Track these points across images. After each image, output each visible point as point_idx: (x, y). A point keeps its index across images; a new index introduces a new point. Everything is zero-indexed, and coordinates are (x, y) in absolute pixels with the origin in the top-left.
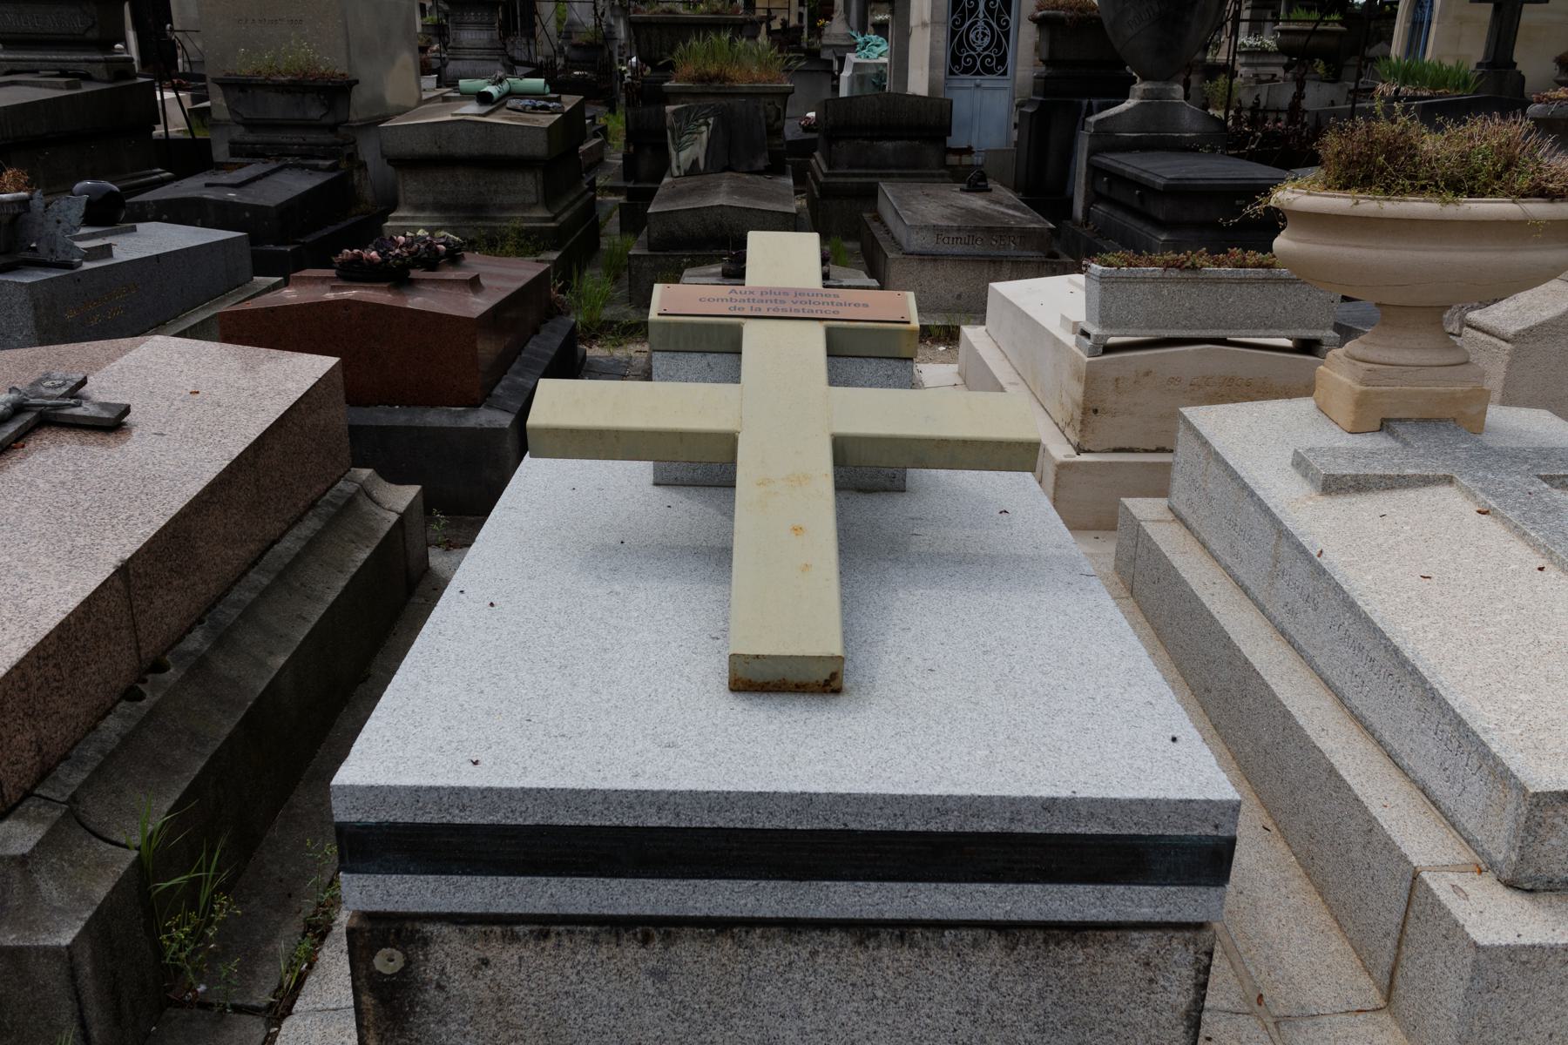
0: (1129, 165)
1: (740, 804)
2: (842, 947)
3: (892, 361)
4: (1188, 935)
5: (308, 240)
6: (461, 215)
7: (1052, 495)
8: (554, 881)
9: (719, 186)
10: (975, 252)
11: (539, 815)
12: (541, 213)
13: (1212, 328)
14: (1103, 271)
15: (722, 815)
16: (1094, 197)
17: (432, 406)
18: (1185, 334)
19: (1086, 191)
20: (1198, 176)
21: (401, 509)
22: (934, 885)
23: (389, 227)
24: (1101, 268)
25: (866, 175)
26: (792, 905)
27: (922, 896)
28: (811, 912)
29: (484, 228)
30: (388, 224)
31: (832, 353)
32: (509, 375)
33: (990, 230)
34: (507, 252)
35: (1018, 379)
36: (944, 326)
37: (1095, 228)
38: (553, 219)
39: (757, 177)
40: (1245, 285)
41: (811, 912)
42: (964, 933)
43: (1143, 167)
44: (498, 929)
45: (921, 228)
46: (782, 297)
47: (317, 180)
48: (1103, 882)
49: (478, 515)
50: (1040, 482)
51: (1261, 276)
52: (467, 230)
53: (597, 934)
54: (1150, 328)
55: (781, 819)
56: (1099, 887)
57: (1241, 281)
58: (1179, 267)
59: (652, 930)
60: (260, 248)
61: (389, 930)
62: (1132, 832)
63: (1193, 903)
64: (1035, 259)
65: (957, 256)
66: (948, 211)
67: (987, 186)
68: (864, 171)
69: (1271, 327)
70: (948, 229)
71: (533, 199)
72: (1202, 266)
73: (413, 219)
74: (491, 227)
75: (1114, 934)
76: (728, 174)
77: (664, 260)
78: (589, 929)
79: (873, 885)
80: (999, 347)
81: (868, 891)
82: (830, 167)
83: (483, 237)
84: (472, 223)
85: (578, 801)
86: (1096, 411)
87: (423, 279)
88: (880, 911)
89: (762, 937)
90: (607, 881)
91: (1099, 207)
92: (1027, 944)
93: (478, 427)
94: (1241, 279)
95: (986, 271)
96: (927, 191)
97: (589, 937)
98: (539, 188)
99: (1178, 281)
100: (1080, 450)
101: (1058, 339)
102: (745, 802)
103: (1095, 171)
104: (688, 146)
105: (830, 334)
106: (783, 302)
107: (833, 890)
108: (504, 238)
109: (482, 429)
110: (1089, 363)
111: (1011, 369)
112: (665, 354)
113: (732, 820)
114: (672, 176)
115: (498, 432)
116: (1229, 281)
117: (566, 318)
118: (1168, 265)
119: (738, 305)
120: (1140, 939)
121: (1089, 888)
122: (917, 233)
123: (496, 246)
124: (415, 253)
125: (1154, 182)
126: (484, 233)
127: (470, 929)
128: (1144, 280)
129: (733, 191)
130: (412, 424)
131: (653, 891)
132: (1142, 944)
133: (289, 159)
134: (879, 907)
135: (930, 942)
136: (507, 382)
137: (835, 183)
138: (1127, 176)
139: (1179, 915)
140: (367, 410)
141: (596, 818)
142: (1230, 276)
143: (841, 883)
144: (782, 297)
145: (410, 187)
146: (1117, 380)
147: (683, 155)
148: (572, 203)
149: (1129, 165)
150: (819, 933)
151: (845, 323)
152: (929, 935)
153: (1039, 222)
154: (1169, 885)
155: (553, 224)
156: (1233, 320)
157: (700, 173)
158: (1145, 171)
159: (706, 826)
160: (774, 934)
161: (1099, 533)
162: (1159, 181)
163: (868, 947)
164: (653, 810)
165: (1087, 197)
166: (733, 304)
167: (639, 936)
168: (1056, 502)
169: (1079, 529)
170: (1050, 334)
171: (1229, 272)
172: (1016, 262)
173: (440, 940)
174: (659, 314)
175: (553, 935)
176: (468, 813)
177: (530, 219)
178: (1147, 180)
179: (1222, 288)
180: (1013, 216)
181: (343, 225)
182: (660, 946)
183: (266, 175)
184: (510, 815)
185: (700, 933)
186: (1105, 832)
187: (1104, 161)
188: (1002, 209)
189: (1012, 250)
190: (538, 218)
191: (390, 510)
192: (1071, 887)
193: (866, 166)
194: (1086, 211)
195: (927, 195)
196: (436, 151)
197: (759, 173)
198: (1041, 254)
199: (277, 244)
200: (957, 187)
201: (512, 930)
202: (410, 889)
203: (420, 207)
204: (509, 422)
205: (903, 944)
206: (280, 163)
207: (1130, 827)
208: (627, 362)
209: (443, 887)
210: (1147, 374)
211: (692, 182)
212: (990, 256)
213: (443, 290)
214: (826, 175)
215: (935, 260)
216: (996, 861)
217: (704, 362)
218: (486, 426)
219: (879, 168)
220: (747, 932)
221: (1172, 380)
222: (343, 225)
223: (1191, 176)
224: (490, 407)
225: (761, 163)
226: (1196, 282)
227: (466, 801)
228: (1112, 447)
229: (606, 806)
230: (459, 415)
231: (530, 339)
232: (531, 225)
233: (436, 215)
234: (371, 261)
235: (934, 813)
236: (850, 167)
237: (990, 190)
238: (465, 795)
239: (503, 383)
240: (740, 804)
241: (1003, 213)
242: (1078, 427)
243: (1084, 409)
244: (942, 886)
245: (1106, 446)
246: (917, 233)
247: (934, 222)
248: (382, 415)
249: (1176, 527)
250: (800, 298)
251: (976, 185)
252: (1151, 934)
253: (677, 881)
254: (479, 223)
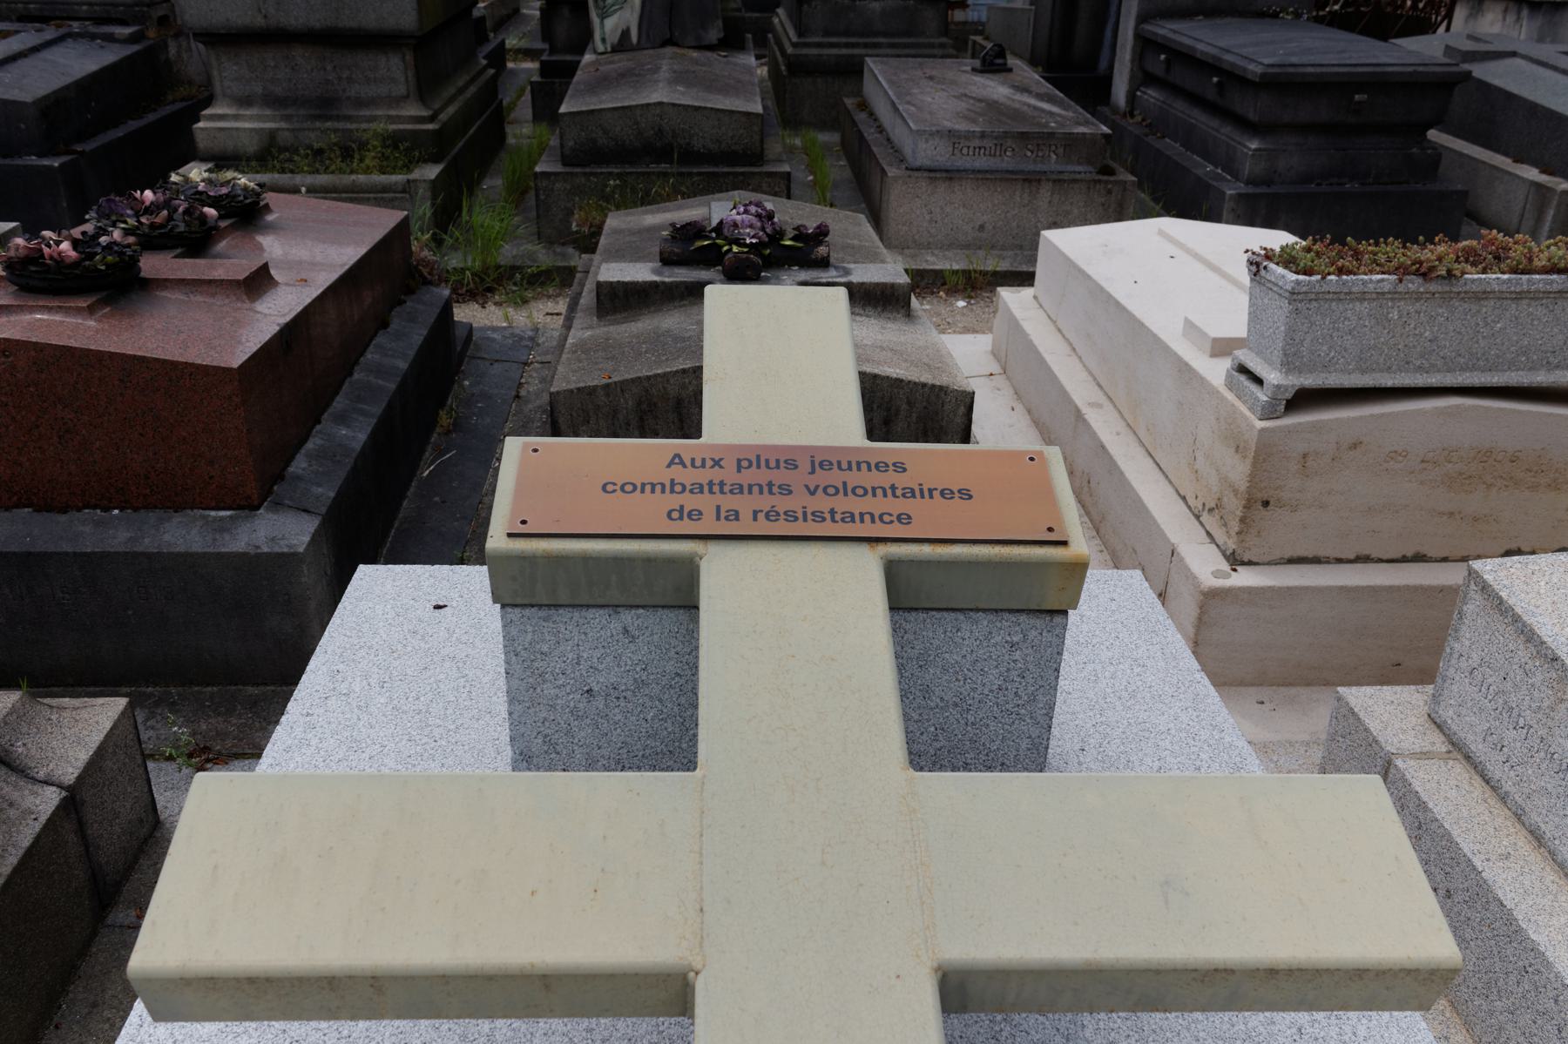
0: (1201, 41)
3: (1023, 618)
5: (89, 146)
6: (302, 112)
7: (1192, 636)
9: (657, 70)
10: (1004, 166)
12: (413, 110)
13: (1462, 369)
14: (1298, 282)
16: (1143, 77)
17: (178, 509)
18: (1420, 380)
19: (1132, 70)
20: (1305, 59)
21: (70, 774)
23: (202, 129)
24: (1294, 277)
25: (847, 45)
29: (335, 131)
30: (201, 124)
31: (897, 605)
32: (326, 424)
33: (1024, 136)
34: (368, 168)
35: (1103, 399)
36: (964, 271)
37: (1143, 120)
38: (432, 119)
39: (709, 54)
40: (1525, 302)
43: (1222, 44)
45: (932, 134)
46: (780, 477)
47: (108, 56)
49: (266, 684)
50: (1162, 596)
51: (1555, 287)
52: (312, 135)
54: (1363, 372)
57: (1518, 296)
58: (1424, 275)
60: (18, 162)
64: (1083, 175)
65: (979, 171)
66: (962, 106)
67: (1005, 64)
68: (844, 40)
69: (1557, 367)
70: (969, 135)
71: (401, 89)
72: (1463, 273)
73: (236, 117)
74: (343, 130)
76: (669, 50)
77: (583, 180)
80: (1059, 330)
82: (800, 35)
83: (335, 144)
84: (318, 124)
86: (1266, 504)
87: (166, 280)
91: (1149, 92)
93: (252, 551)
94: (1520, 293)
95: (1017, 193)
96: (929, 72)
98: (410, 74)
99: (1418, 297)
100: (1235, 561)
101: (1187, 364)
103: (1145, 44)
104: (615, 11)
105: (893, 573)
106: (786, 490)
108: (363, 146)
109: (258, 556)
110: (1263, 430)
111: (1085, 374)
112: (527, 612)
114: (595, 52)
115: (285, 561)
116: (1501, 296)
117: (435, 290)
118: (1402, 271)
119: (690, 502)
122: (927, 141)
123: (352, 157)
124: (162, 226)
125: (1245, 69)
126: (333, 138)
128: (1362, 297)
129: (679, 78)
130: (139, 549)
133: (75, 24)
136: (319, 442)
137: (806, 55)
138: (1198, 56)
140: (63, 518)
142: (1504, 288)
144: (780, 477)
145: (229, 72)
146: (1305, 456)
147: (610, 23)
148: (461, 91)
149: (1201, 41)
151: (927, 550)
153: (1086, 123)
155: (430, 127)
156: (1498, 356)
157: (633, 49)
158: (1228, 51)
161: (1264, 694)
162: (1251, 67)
165: (1132, 78)
166: (674, 501)
168: (1197, 646)
169: (1231, 685)
170: (1166, 349)
171: (1504, 282)
172: (1059, 180)
174: (510, 535)
177: (398, 120)
178: (1233, 64)
179: (1488, 306)
180: (1051, 114)
181: (151, 117)
183: (35, 50)
187: (1161, 32)
188: (1033, 101)
189: (1053, 163)
190: (411, 117)
191: (47, 783)
193: (847, 33)
194: (1131, 97)
195: (931, 78)
196: (259, 21)
197: (710, 48)
198: (1091, 169)
199: (41, 155)
200: (968, 63)
203: (245, 101)
204: (306, 539)
206: (62, 31)
208: (532, 339)
210: (1354, 446)
211: (622, 62)
212: (1022, 172)
213: (199, 298)
214: (794, 45)
215: (951, 179)
217: (615, 626)
218: (265, 549)
219: (862, 35)
221: (1394, 455)
222: (151, 117)
223: (1294, 60)
224: (278, 505)
225: (714, 35)
226: (1446, 298)
228: (1286, 557)
230: (222, 527)
231: (371, 341)
232: (401, 127)
233: (268, 112)
234: (60, 261)
236: (827, 33)
237: (1010, 70)
239: (310, 445)
241: (1035, 108)
242: (1235, 526)
243: (1249, 500)
245: (1277, 555)
246: (927, 141)
247: (948, 124)
248: (87, 529)
249: (1459, 769)
250: (822, 478)
251: (992, 64)
254: (329, 124)
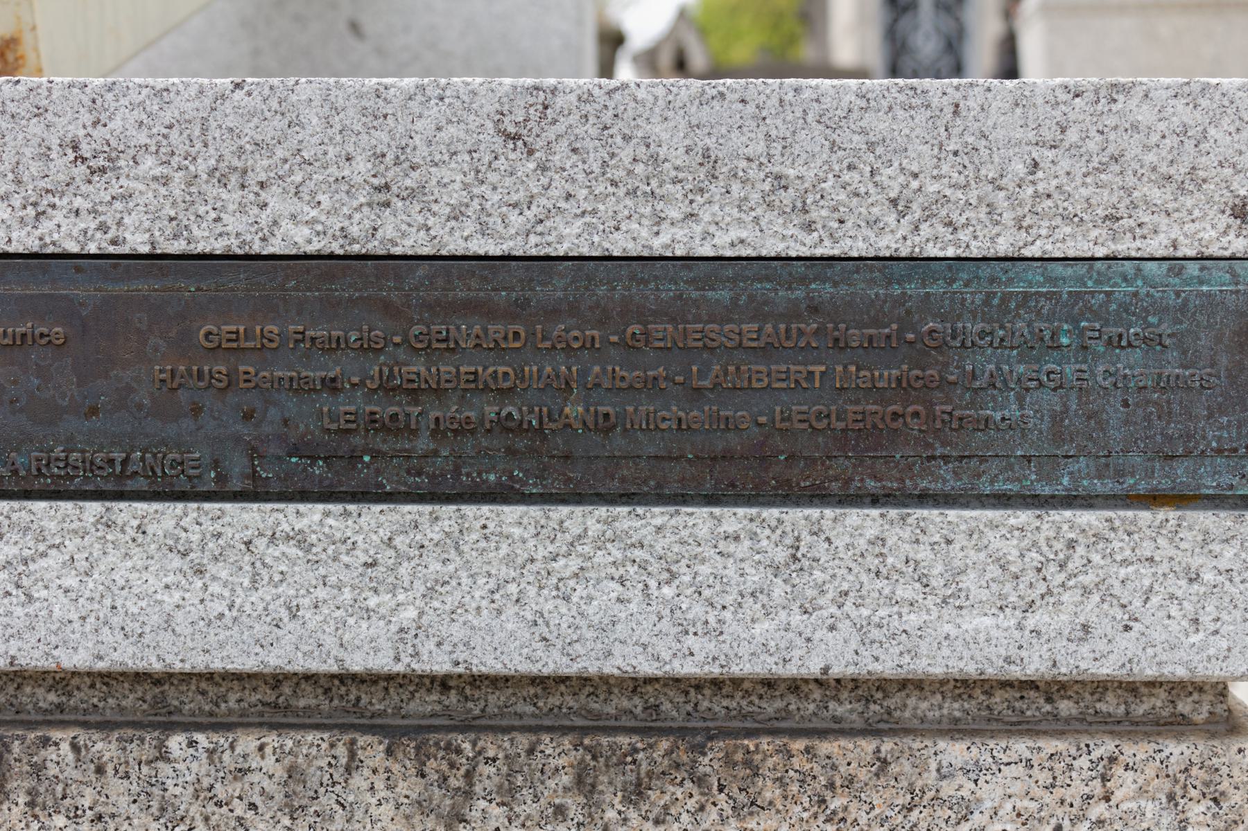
4: (1177, 751)
22: (94, 508)
27: (54, 560)
42: (247, 742)
48: (789, 496)
56: (772, 513)
62: (886, 244)
63: (1180, 586)
75: (868, 746)
92: (507, 794)
120: (975, 772)
121: (734, 518)
132: (990, 793)
135: (116, 786)
139: (1126, 644)
152: (105, 747)
154: (1069, 501)
186: (772, 247)
192: (658, 515)
207: (872, 223)
216: (332, 385)
235: (60, 165)
244: (126, 512)
252: (1021, 747)
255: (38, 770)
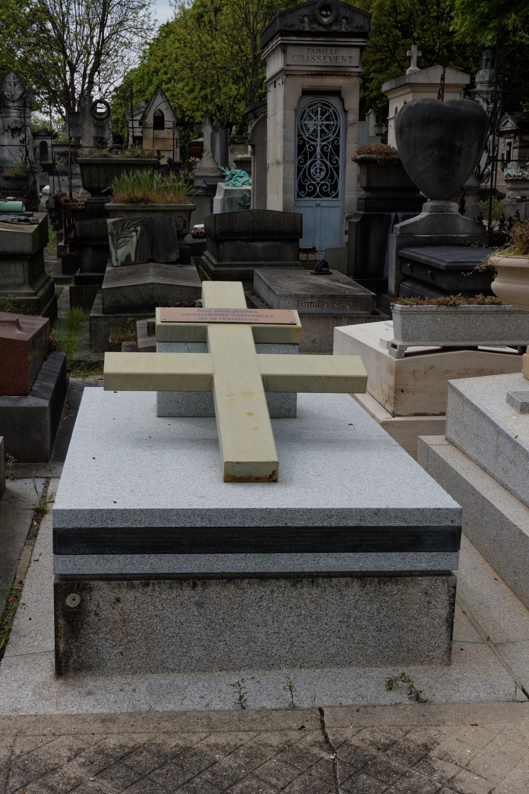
1: (239, 514)
2: (285, 587)
3: (287, 346)
4: (444, 578)
8: (153, 556)
9: (148, 271)
10: (324, 311)
11: (147, 522)
12: (26, 290)
13: (468, 340)
14: (402, 308)
15: (230, 520)
16: (402, 277)
18: (453, 344)
19: (396, 273)
22: (327, 554)
24: (401, 306)
25: (244, 266)
26: (262, 566)
27: (322, 560)
28: (271, 569)
38: (35, 294)
39: (172, 266)
40: (485, 315)
41: (271, 569)
42: (341, 579)
43: (432, 256)
44: (125, 583)
45: (287, 297)
48: (403, 551)
49: (27, 462)
51: (494, 309)
53: (171, 584)
54: (432, 341)
55: (257, 522)
56: (401, 553)
57: (483, 313)
58: (446, 305)
59: (198, 582)
61: (74, 584)
62: (415, 525)
63: (445, 560)
66: (304, 286)
67: (328, 271)
68: (242, 263)
69: (502, 339)
70: (305, 297)
71: (21, 280)
72: (459, 304)
75: (410, 578)
76: (152, 264)
77: (114, 320)
78: (168, 581)
79: (299, 554)
81: (297, 558)
82: (218, 261)
85: (165, 515)
86: (402, 391)
88: (303, 568)
89: (248, 583)
90: (177, 555)
91: (406, 284)
92: (370, 584)
93: (29, 406)
94: (482, 311)
96: (288, 275)
97: (168, 585)
98: (26, 273)
99: (446, 313)
101: (378, 352)
102: (241, 513)
103: (401, 260)
104: (123, 246)
107: (280, 557)
109: (31, 408)
110: (397, 362)
112: (164, 343)
113: (235, 523)
114: (112, 266)
116: (477, 313)
118: (439, 304)
120: (422, 580)
121: (397, 554)
122: (284, 300)
125: (439, 265)
127: (113, 583)
128: (426, 313)
129: (158, 274)
131: (198, 560)
132: (423, 583)
134: (302, 566)
135: (326, 584)
137: (222, 271)
138: (422, 262)
139: (439, 567)
141: (173, 523)
142: (476, 309)
143: (285, 554)
146: (414, 372)
147: (120, 252)
148: (43, 285)
150: (274, 580)
151: (262, 325)
152: (325, 580)
153: (365, 292)
154: (433, 551)
155: (35, 298)
156: (480, 335)
157: (132, 264)
158: (434, 258)
159: (223, 526)
160: (253, 582)
163: (297, 588)
164: (199, 519)
165: (397, 278)
166: (201, 317)
167: (191, 584)
171: (475, 307)
173: (98, 588)
174: (162, 322)
175: (151, 584)
176: (114, 522)
177: (19, 294)
180: (348, 289)
182: (201, 589)
184: (134, 522)
185: (220, 582)
186: (403, 525)
187: (407, 253)
188: (340, 285)
189: (348, 310)
190: (26, 293)
192: (389, 554)
193: (244, 259)
194: (397, 288)
195: (289, 277)
197: (173, 263)
198: (367, 312)
200: (309, 272)
201: (132, 583)
202: (85, 562)
205: (313, 585)
207: (414, 523)
209: (101, 561)
210: (432, 368)
211: (127, 269)
212: (333, 314)
214: (215, 266)
216: (354, 540)
219: (252, 260)
220: (241, 581)
223: (462, 260)
225: (174, 256)
226: (457, 313)
227: (114, 516)
228: (414, 413)
229: (178, 517)
230: (16, 400)
232: (21, 298)
235: (325, 517)
236: (233, 260)
237: (331, 273)
238: (114, 513)
240: (239, 514)
241: (340, 287)
242: (393, 401)
243: (396, 390)
244: (330, 554)
245: (410, 412)
246: (284, 300)
247: (296, 293)
250: (236, 313)
251: (321, 270)
252: (427, 578)
253: (209, 555)
255: (317, 583)
